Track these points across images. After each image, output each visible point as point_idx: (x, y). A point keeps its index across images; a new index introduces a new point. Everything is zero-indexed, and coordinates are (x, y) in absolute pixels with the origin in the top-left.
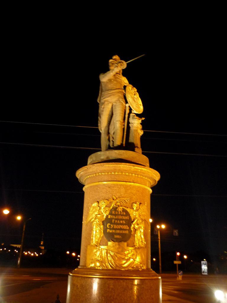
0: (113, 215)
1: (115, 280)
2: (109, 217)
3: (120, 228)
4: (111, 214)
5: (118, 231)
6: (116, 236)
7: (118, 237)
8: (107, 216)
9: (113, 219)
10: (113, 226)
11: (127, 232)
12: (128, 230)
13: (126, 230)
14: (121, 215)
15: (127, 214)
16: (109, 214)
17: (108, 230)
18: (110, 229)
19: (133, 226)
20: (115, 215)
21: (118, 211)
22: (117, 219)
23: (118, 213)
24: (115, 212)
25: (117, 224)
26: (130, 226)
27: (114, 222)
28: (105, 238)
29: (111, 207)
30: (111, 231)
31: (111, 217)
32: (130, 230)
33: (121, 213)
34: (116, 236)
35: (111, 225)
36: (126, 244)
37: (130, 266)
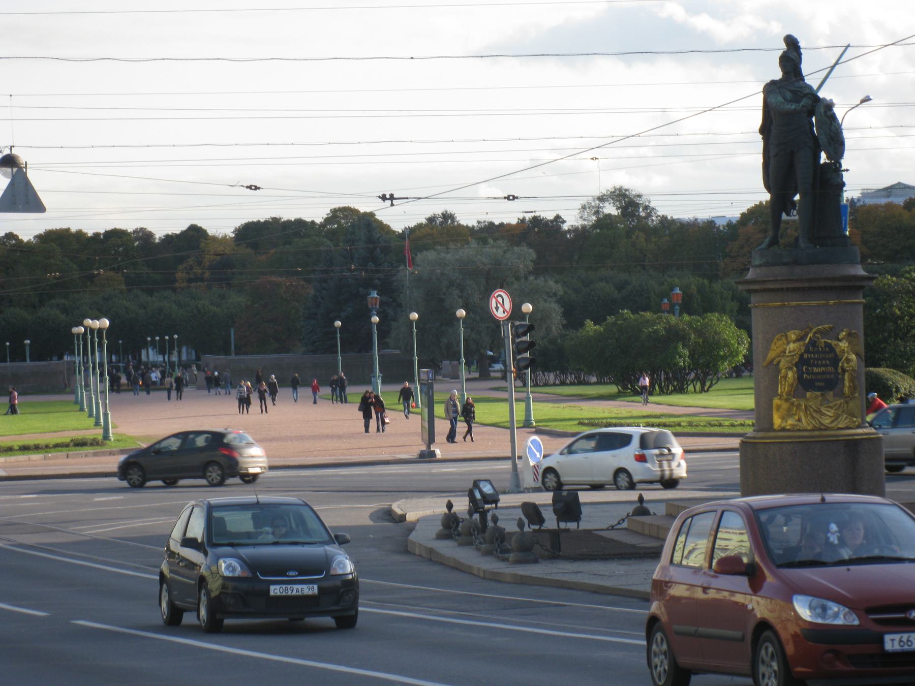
0: (811, 353)
4: (807, 351)
6: (817, 384)
7: (821, 384)
8: (802, 355)
9: (811, 358)
10: (813, 370)
11: (832, 376)
13: (830, 373)
15: (832, 349)
16: (805, 352)
17: (805, 376)
18: (808, 374)
19: (840, 364)
21: (818, 347)
22: (818, 359)
23: (818, 350)
24: (813, 349)
25: (817, 366)
26: (836, 366)
27: (814, 363)
28: (800, 387)
31: (808, 356)
32: (837, 373)
34: (817, 384)
36: (831, 393)
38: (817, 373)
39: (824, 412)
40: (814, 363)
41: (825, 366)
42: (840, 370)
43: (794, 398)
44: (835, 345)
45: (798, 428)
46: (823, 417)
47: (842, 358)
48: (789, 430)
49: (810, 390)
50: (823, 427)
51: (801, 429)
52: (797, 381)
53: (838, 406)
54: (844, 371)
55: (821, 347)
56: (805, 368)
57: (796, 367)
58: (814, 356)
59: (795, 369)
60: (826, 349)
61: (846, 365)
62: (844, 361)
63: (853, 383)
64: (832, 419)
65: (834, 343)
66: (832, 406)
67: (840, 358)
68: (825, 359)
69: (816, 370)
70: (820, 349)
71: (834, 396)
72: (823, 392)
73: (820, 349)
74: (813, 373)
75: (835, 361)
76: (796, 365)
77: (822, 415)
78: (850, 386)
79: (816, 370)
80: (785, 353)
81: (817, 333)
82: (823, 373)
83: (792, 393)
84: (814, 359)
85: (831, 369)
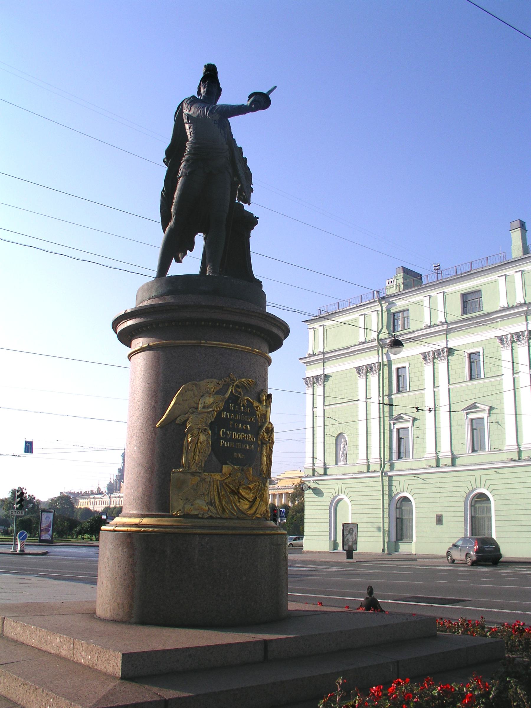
2: (224, 415)
3: (242, 439)
4: (226, 409)
5: (239, 445)
7: (240, 456)
8: (219, 414)
9: (233, 420)
12: (253, 442)
13: (250, 443)
16: (224, 410)
20: (235, 412)
21: (239, 405)
22: (238, 421)
23: (240, 409)
25: (239, 431)
27: (233, 425)
28: (214, 459)
29: (227, 395)
30: (227, 445)
31: (227, 416)
33: (244, 409)
35: (228, 432)
37: (257, 512)
38: (237, 441)
39: (243, 494)
40: (233, 425)
41: (246, 431)
43: (204, 472)
44: (257, 407)
45: (211, 514)
46: (241, 500)
48: (196, 517)
50: (242, 516)
51: (214, 516)
52: (210, 448)
55: (243, 406)
56: (223, 431)
57: (211, 429)
58: (235, 416)
59: (210, 432)
65: (256, 403)
68: (247, 423)
69: (235, 435)
70: (242, 408)
73: (242, 408)
74: (231, 440)
76: (212, 426)
77: (240, 498)
79: (235, 435)
80: (197, 408)
81: (239, 388)
82: (244, 441)
83: (203, 465)
84: (235, 421)
85: (251, 438)
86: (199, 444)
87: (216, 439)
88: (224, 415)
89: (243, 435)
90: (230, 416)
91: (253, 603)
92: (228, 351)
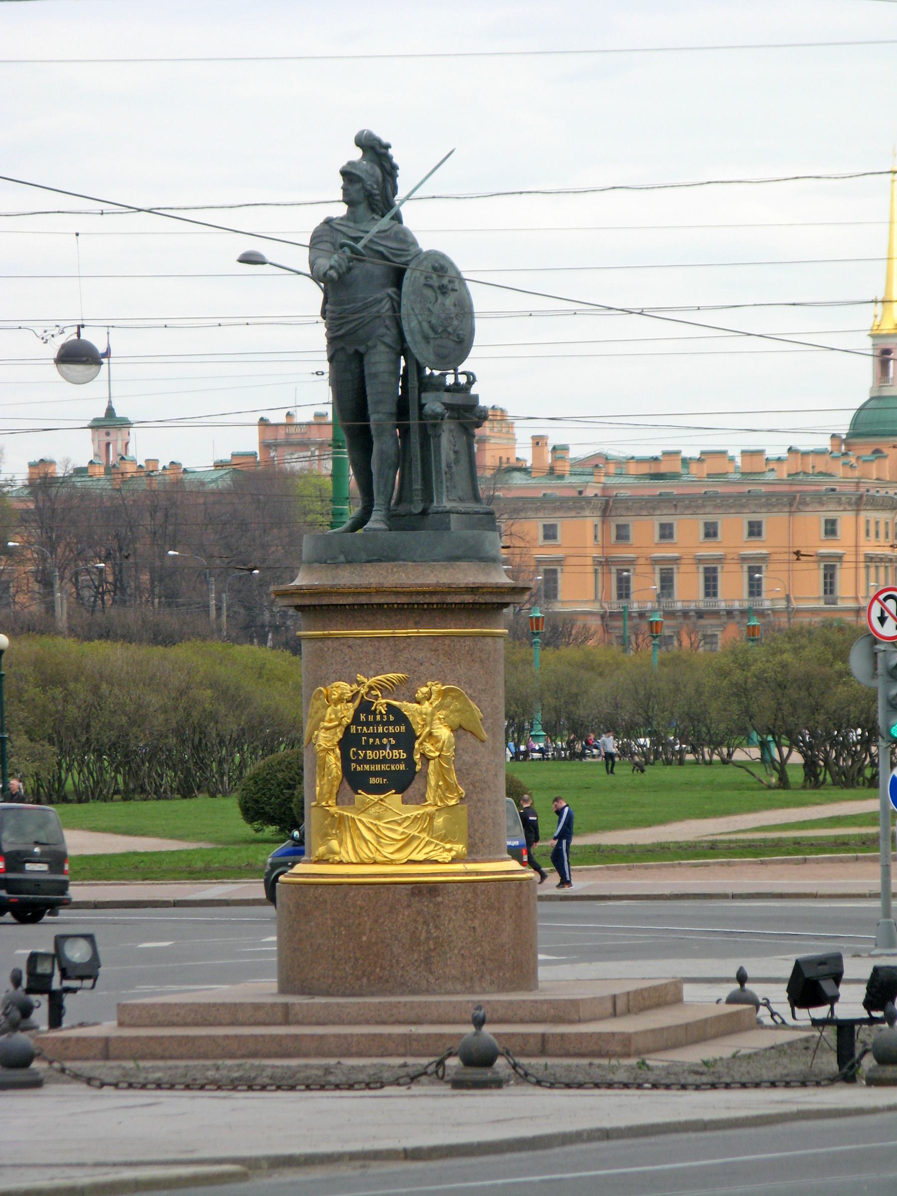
0: (363, 724)
1: (367, 887)
4: (356, 720)
6: (373, 781)
8: (348, 728)
9: (365, 735)
10: (366, 754)
11: (402, 767)
14: (384, 724)
17: (353, 765)
19: (417, 746)
20: (367, 724)
23: (375, 718)
25: (373, 747)
26: (410, 751)
27: (367, 741)
30: (359, 769)
31: (357, 730)
32: (410, 762)
33: (382, 718)
35: (360, 752)
40: (367, 741)
42: (417, 757)
46: (382, 840)
47: (420, 736)
49: (360, 791)
53: (411, 820)
54: (426, 759)
60: (388, 718)
61: (428, 746)
62: (424, 740)
63: (445, 780)
64: (401, 843)
66: (400, 821)
67: (418, 734)
68: (388, 735)
69: (370, 754)
70: (378, 717)
71: (404, 802)
72: (382, 796)
73: (378, 717)
74: (365, 761)
75: (407, 740)
78: (438, 786)
84: (369, 735)
86: (326, 770)
87: (345, 760)
88: (353, 729)
89: (383, 753)
90: (362, 730)
91: (378, 970)
92: (358, 641)
